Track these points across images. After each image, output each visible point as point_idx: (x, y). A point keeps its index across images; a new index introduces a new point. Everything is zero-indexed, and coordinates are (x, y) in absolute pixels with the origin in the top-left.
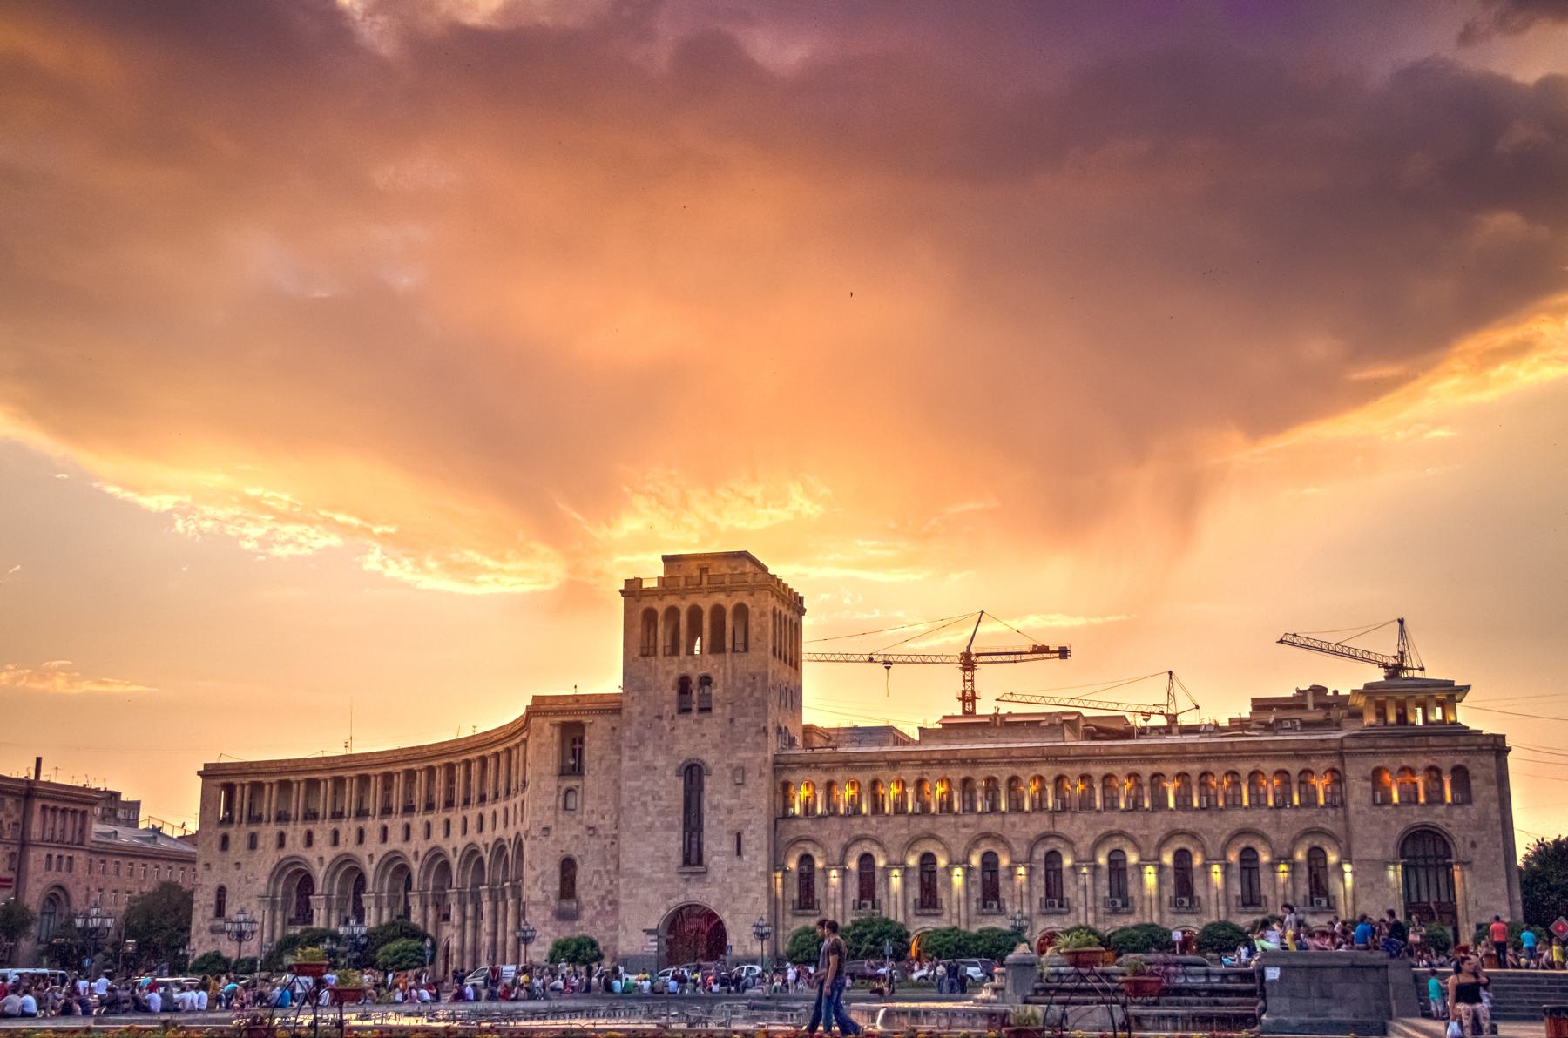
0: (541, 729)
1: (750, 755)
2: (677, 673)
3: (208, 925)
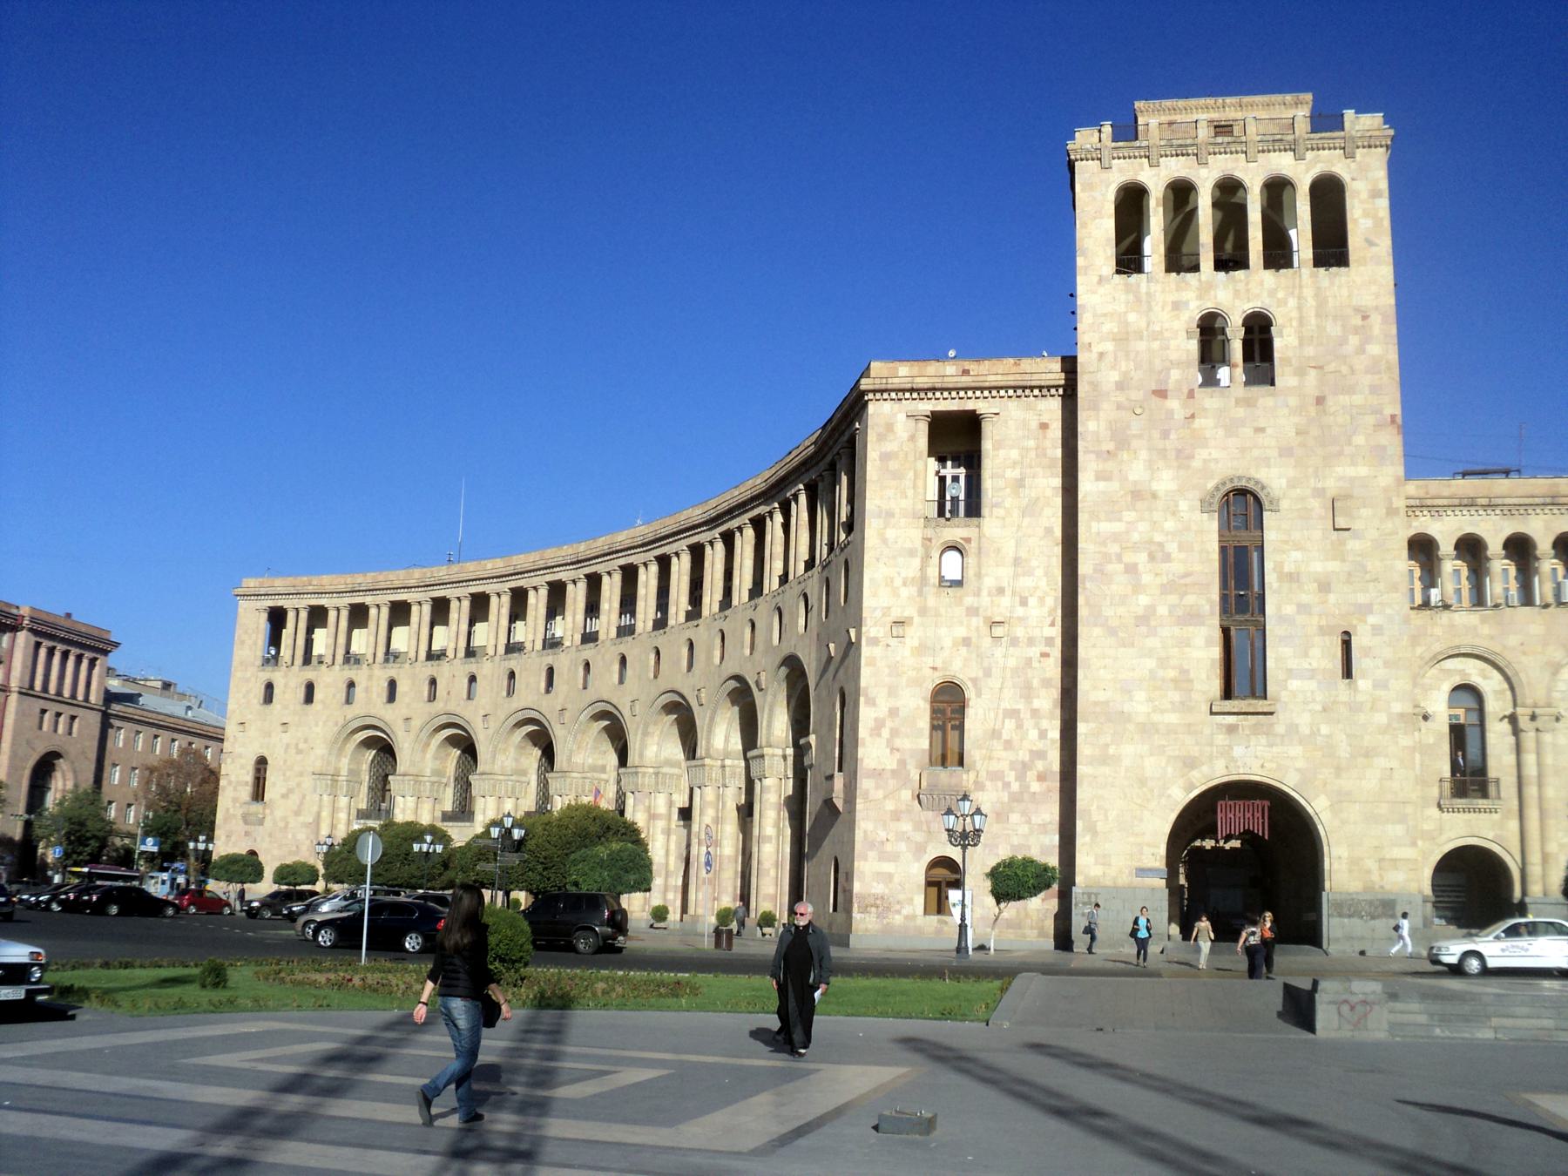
0: (890, 427)
1: (1363, 471)
3: (239, 812)
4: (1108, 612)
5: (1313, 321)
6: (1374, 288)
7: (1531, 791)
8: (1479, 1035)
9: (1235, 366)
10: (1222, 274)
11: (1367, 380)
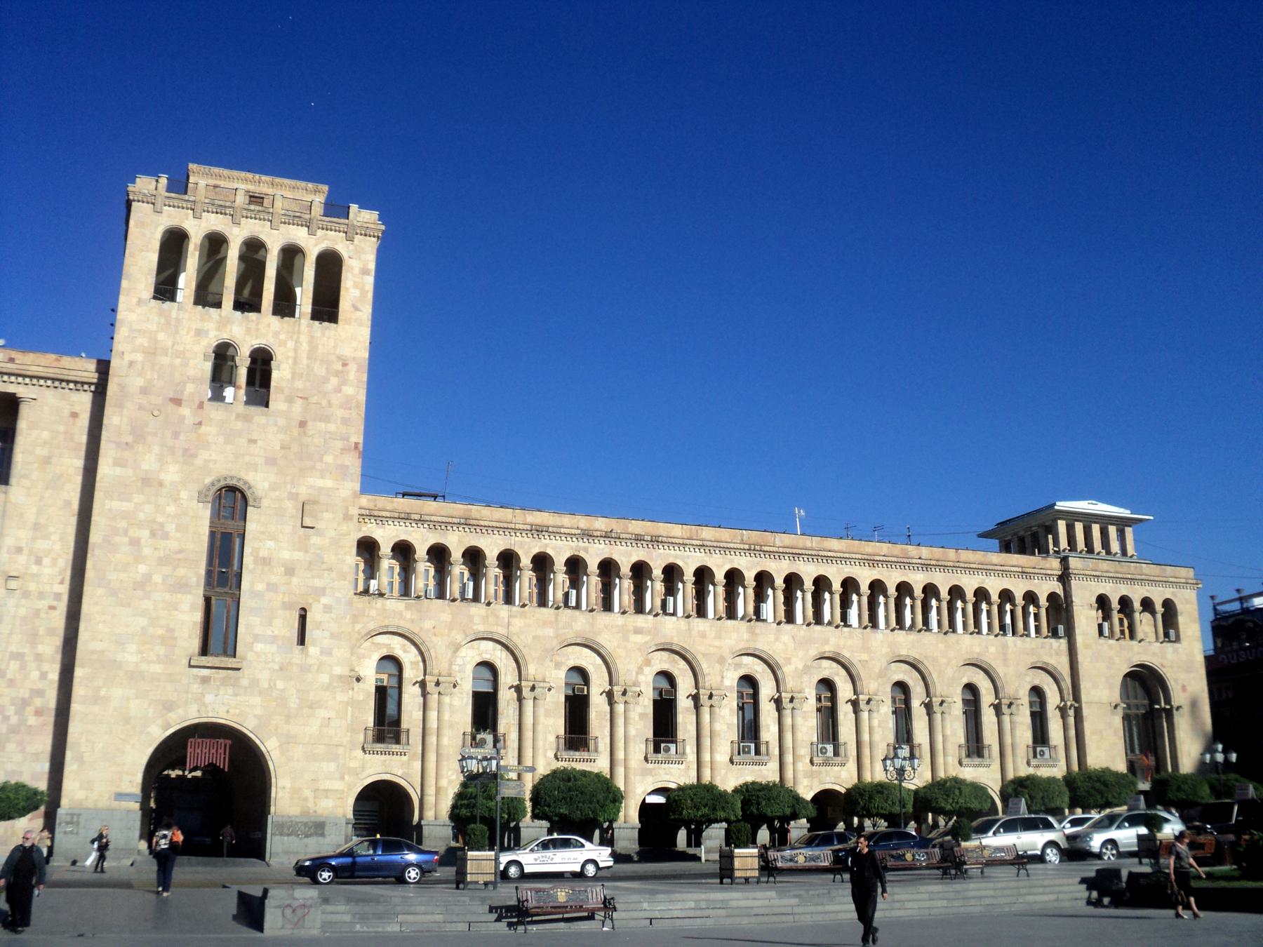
1: (329, 483)
4: (112, 576)
5: (305, 362)
6: (355, 344)
7: (432, 740)
8: (389, 929)
9: (239, 388)
10: (239, 313)
11: (340, 413)
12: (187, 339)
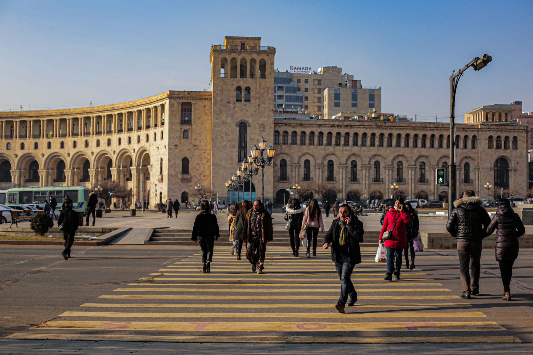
1: (266, 119)
2: (236, 85)
5: (258, 89)
12: (230, 86)
